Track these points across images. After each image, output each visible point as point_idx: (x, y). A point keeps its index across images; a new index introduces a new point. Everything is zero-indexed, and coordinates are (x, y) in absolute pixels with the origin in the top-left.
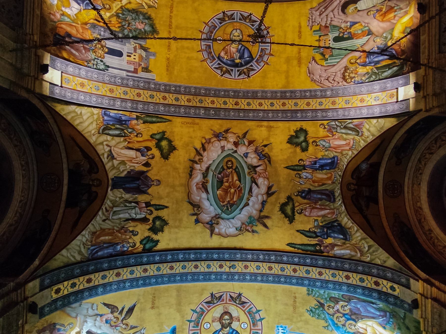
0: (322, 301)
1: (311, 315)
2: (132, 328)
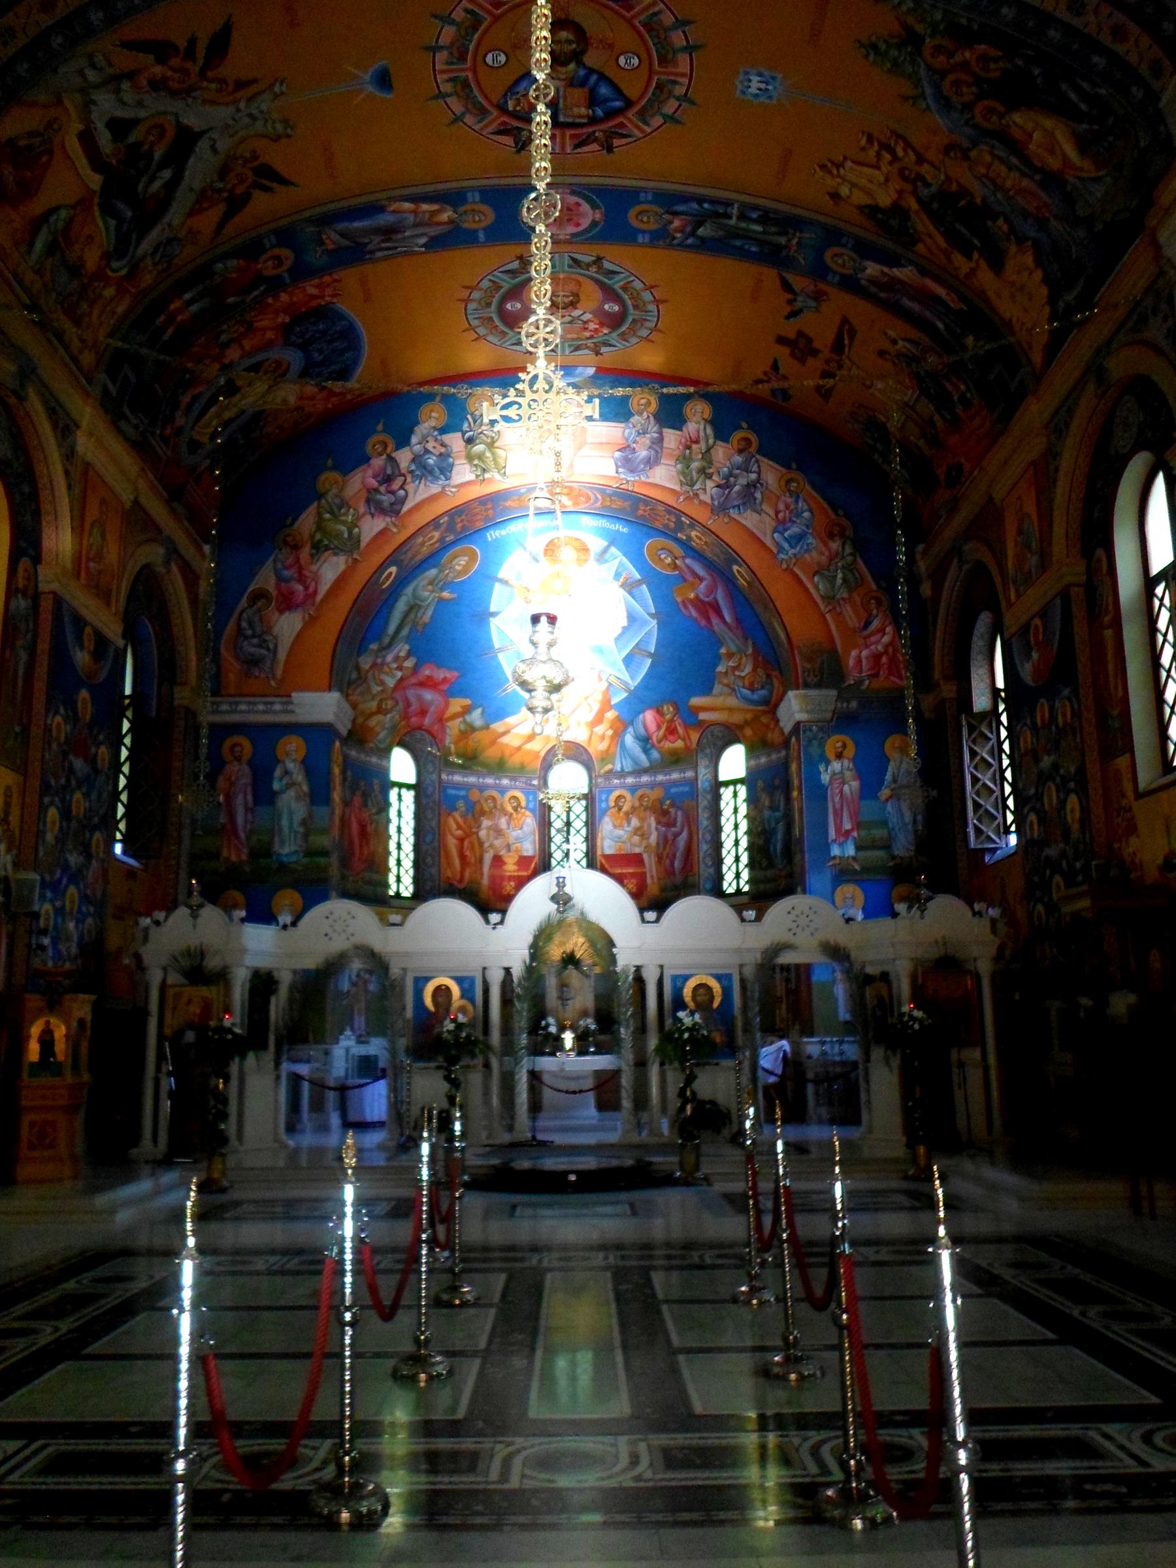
0: (919, 28)
1: (871, 58)
2: (240, 85)
